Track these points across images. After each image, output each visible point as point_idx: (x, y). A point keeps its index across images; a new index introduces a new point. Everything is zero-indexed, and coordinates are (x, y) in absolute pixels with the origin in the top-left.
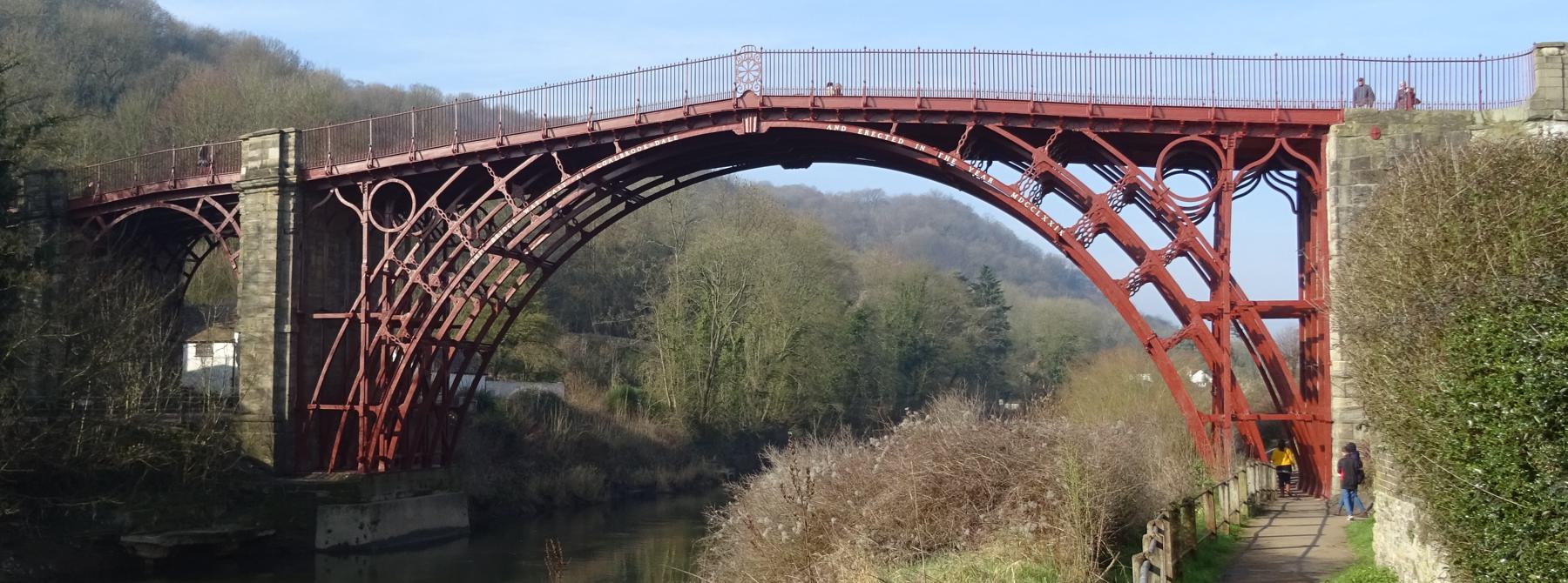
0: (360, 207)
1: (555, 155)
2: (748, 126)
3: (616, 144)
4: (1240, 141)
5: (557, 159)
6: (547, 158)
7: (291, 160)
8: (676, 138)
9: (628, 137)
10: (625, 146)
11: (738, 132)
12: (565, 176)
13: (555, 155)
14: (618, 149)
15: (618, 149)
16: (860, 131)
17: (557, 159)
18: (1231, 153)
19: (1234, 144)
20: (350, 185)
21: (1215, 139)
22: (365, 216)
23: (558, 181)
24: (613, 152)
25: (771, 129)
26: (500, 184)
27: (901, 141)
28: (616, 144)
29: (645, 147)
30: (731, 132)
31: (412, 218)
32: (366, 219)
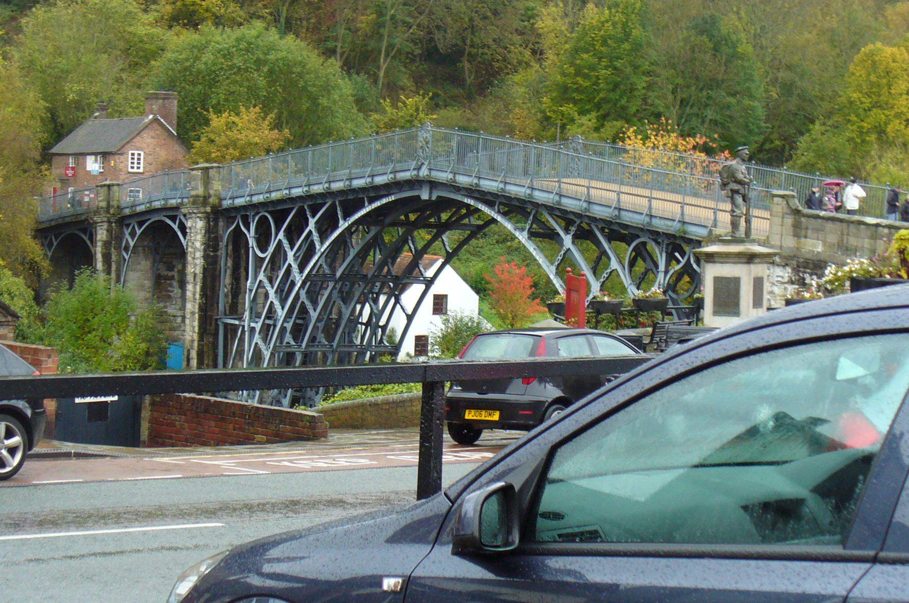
0: (249, 230)
1: (337, 203)
2: (425, 196)
4: (670, 247)
5: (338, 208)
6: (333, 207)
7: (212, 192)
8: (392, 198)
9: (372, 194)
10: (371, 201)
12: (341, 222)
13: (337, 203)
14: (366, 204)
18: (664, 255)
19: (664, 249)
20: (243, 212)
22: (252, 242)
23: (336, 227)
24: (362, 206)
25: (439, 197)
26: (312, 222)
29: (379, 204)
31: (271, 249)
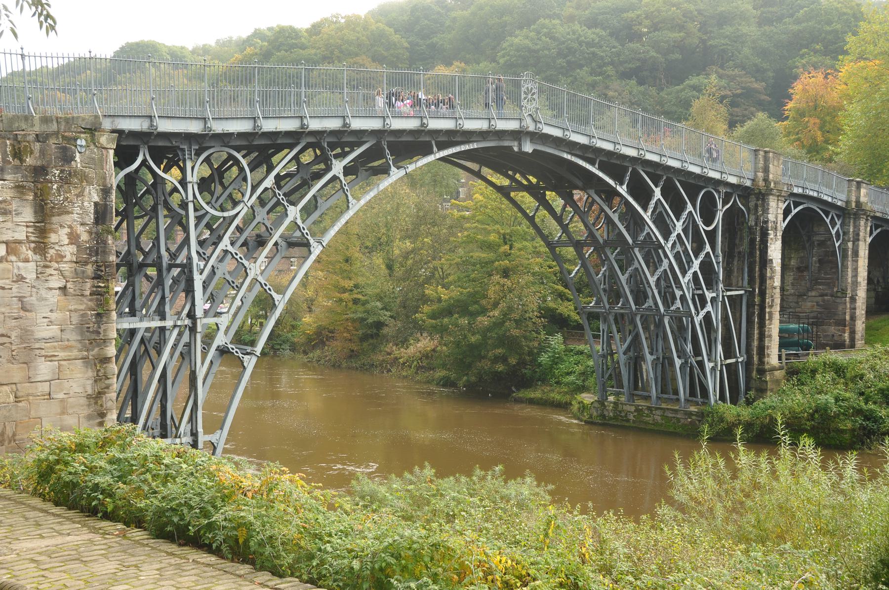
2: (528, 148)
3: (433, 143)
8: (475, 146)
10: (442, 146)
11: (516, 149)
14: (435, 149)
15: (435, 149)
16: (581, 163)
17: (387, 151)
21: (718, 192)
24: (431, 152)
25: (534, 150)
27: (601, 174)
28: (433, 143)
30: (510, 148)
32: (191, 198)
